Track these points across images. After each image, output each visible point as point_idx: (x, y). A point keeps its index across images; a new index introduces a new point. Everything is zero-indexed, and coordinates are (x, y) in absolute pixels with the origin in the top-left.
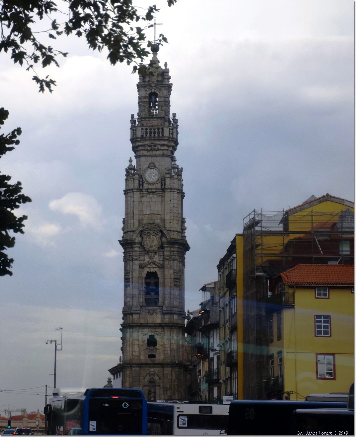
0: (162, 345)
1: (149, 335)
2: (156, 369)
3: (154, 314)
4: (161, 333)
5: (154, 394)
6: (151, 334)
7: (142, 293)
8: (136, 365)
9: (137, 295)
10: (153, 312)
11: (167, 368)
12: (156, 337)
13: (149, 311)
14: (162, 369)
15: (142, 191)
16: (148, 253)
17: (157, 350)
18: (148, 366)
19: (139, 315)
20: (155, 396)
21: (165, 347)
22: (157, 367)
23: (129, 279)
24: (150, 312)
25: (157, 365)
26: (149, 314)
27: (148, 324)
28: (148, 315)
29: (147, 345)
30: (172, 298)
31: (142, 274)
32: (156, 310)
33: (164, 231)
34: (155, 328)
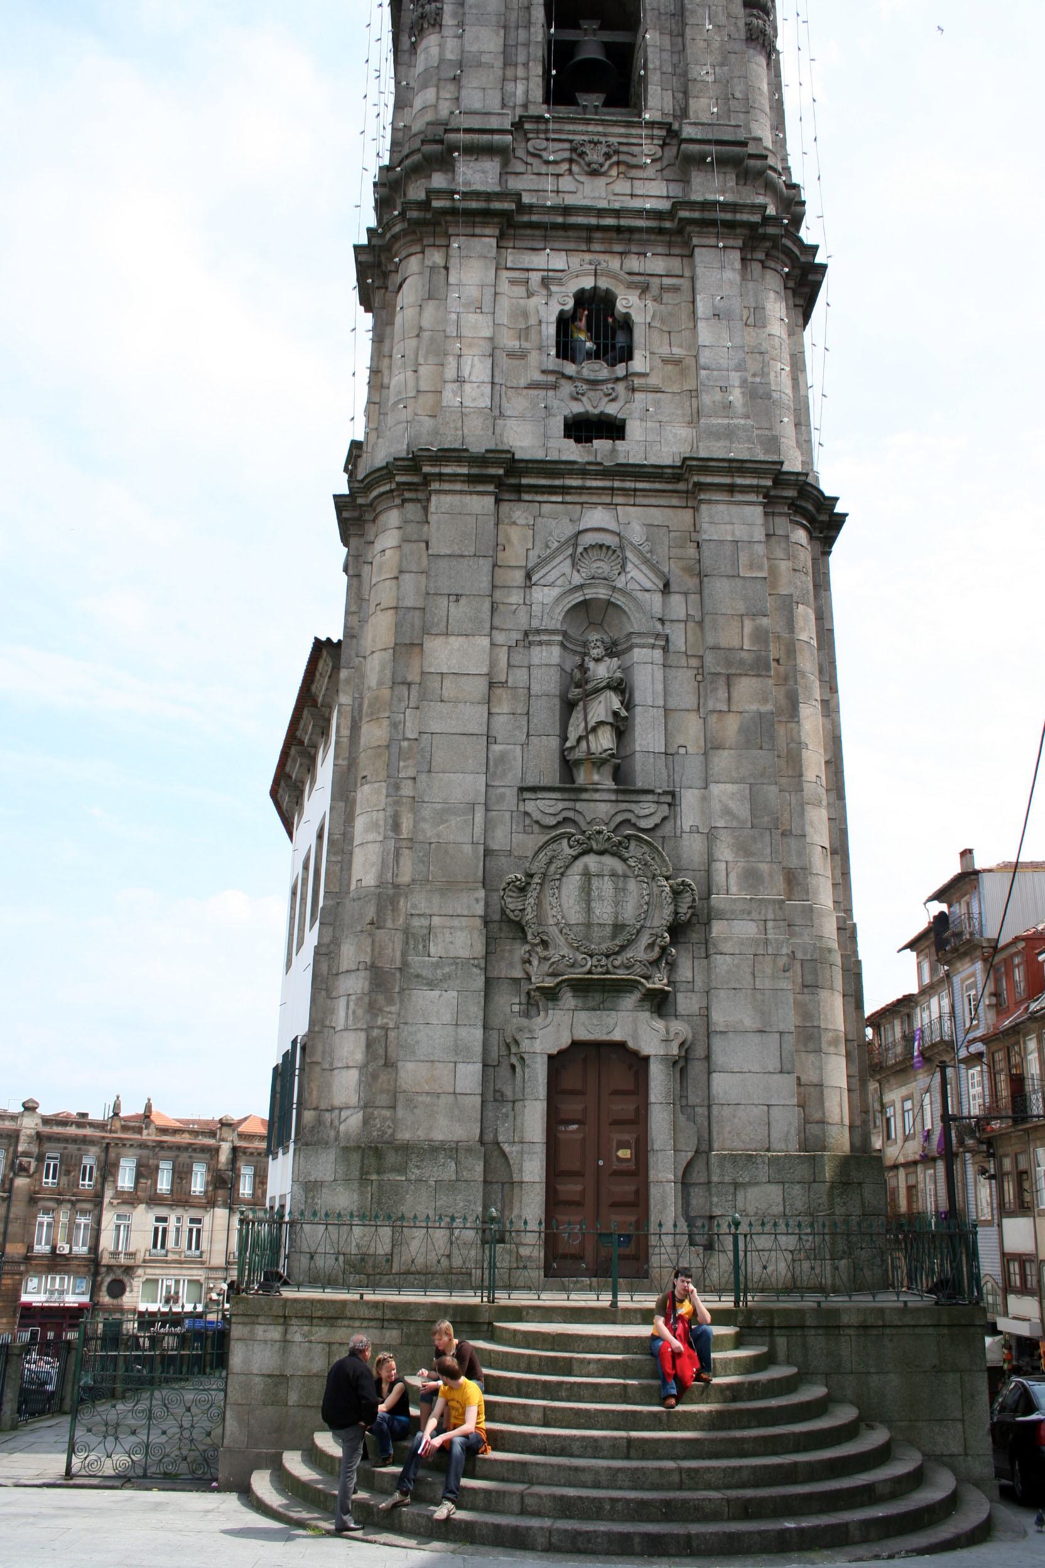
0: (677, 362)
1: (574, 286)
2: (635, 520)
3: (614, 172)
4: (667, 281)
5: (616, 703)
6: (588, 283)
7: (521, 59)
8: (465, 470)
10: (608, 156)
11: (721, 507)
12: (627, 302)
13: (573, 150)
14: (687, 515)
17: (633, 390)
18: (564, 490)
19: (505, 164)
20: (624, 713)
21: (702, 361)
22: (639, 500)
24: (582, 155)
25: (640, 485)
26: (575, 168)
27: (567, 210)
28: (570, 178)
29: (553, 352)
30: (738, 95)
34: (618, 248)
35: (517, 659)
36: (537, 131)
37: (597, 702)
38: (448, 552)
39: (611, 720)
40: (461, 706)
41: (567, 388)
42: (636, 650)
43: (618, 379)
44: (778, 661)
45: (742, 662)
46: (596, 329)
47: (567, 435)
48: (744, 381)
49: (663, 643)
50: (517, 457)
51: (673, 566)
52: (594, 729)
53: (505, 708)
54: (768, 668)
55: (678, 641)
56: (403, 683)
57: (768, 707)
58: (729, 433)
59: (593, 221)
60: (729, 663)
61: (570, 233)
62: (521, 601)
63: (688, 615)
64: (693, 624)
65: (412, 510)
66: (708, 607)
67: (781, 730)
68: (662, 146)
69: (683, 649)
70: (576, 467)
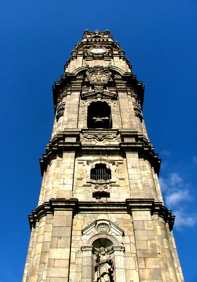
3: (105, 140)
4: (119, 161)
6: (99, 162)
8: (64, 204)
9: (73, 119)
10: (103, 137)
12: (109, 166)
13: (95, 136)
15: (87, 58)
16: (93, 86)
20: (112, 270)
23: (64, 109)
24: (97, 137)
26: (95, 139)
27: (93, 147)
29: (90, 177)
31: (83, 103)
32: (106, 135)
33: (117, 69)
35: (78, 256)
36: (86, 132)
37: (103, 266)
38: (58, 226)
39: (108, 272)
40: (60, 269)
41: (94, 186)
42: (115, 252)
43: (107, 184)
44: (159, 254)
45: (148, 254)
46: (100, 172)
47: (93, 197)
48: (142, 182)
49: (123, 250)
50: (79, 201)
51: (125, 229)
52: (102, 276)
53: (75, 270)
54: (157, 255)
55: (128, 249)
56: (43, 263)
57: (158, 267)
58: (139, 194)
59: (100, 149)
60: (144, 254)
61: (94, 152)
62: (80, 240)
63: (130, 242)
64: (132, 244)
65: (49, 216)
66: (136, 239)
67: (163, 275)
68: (117, 135)
69: (130, 252)
70: (96, 203)
